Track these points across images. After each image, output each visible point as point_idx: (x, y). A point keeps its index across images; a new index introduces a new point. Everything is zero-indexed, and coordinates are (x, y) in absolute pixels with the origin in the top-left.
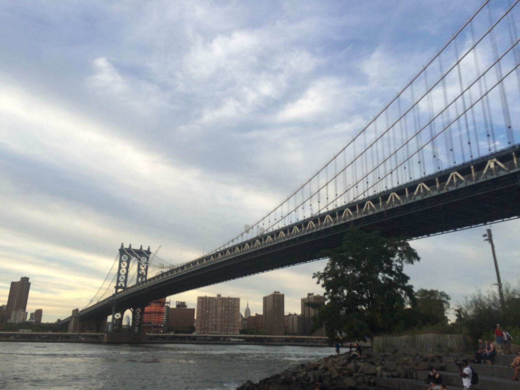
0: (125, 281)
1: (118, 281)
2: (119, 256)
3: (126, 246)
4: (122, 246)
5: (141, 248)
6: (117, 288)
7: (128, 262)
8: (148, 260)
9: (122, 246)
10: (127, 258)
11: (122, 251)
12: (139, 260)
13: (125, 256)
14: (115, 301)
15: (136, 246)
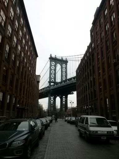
0: (55, 78)
1: (50, 78)
2: (49, 62)
3: (53, 56)
6: (50, 82)
7: (55, 66)
11: (52, 59)
14: (51, 91)
15: (59, 56)
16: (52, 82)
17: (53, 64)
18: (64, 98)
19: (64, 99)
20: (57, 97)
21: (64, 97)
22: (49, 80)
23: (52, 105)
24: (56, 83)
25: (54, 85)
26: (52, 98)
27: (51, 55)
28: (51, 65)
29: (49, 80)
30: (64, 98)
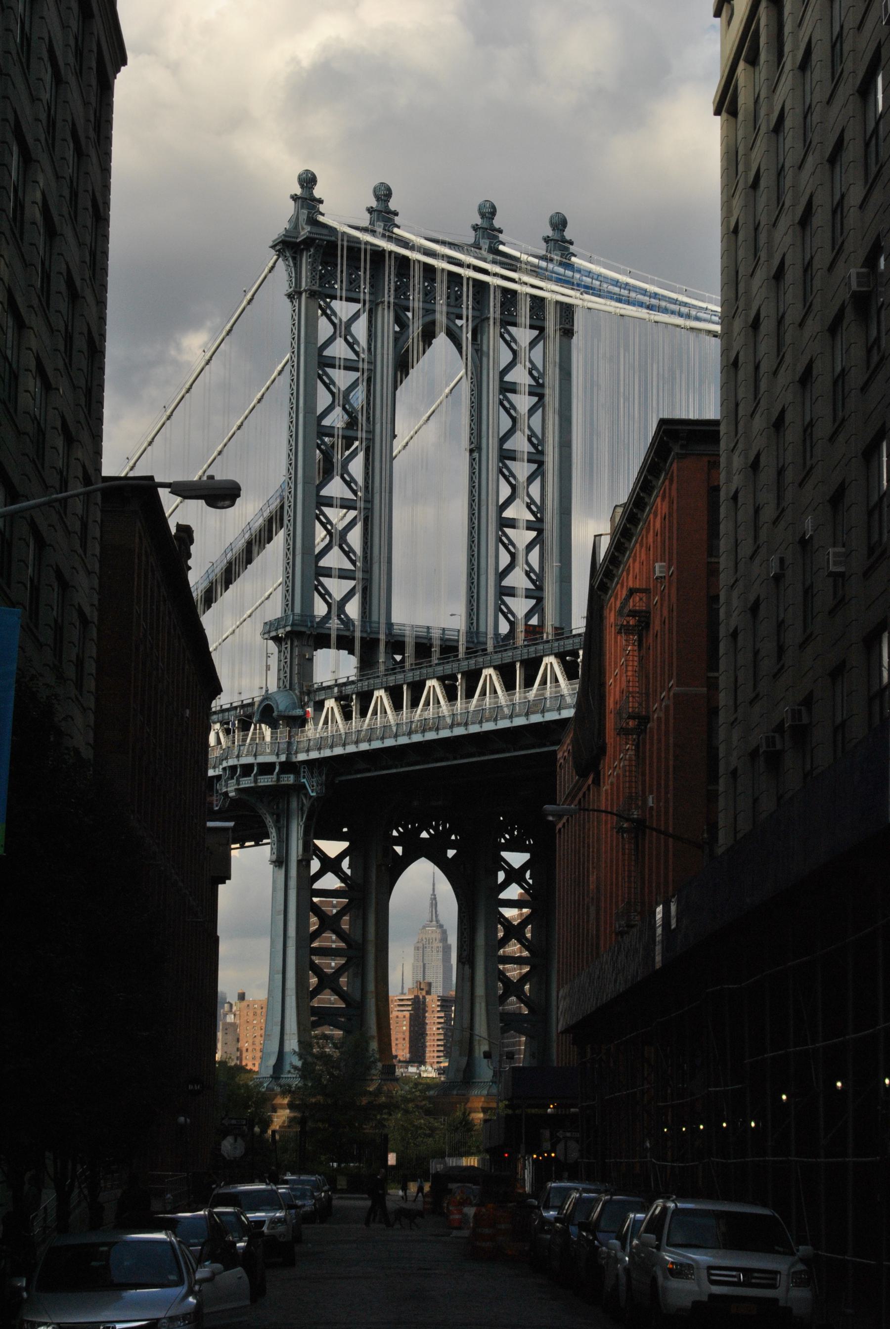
13: (343, 309)
16: (322, 641)
17: (344, 330)
18: (514, 876)
19: (513, 892)
20: (400, 865)
21: (516, 859)
22: (289, 603)
23: (328, 999)
24: (397, 645)
25: (365, 697)
26: (330, 882)
27: (308, 181)
29: (275, 610)
30: (514, 876)
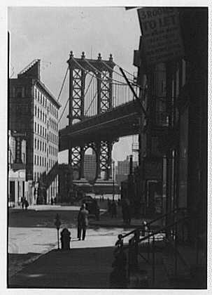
0: (82, 108)
1: (71, 108)
3: (77, 56)
4: (71, 55)
5: (100, 57)
6: (70, 117)
7: (83, 79)
8: (111, 75)
9: (71, 55)
10: (80, 74)
11: (72, 63)
12: (98, 76)
13: (77, 71)
28: (71, 78)
